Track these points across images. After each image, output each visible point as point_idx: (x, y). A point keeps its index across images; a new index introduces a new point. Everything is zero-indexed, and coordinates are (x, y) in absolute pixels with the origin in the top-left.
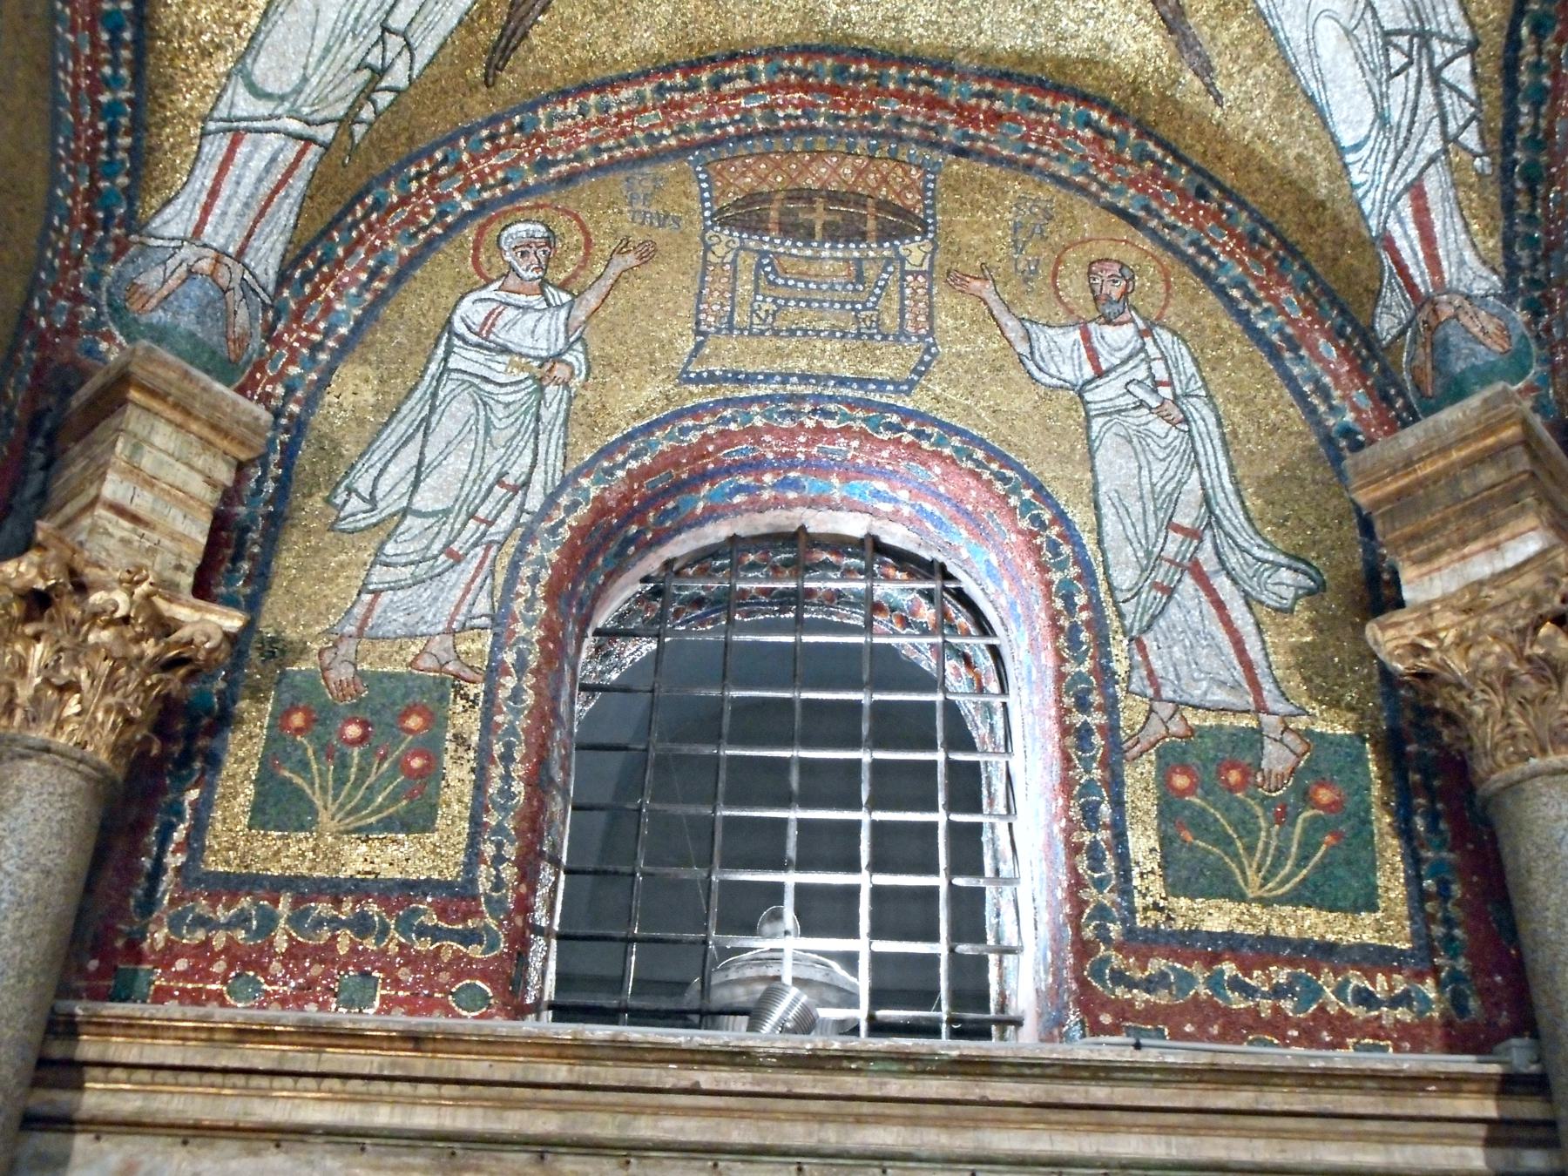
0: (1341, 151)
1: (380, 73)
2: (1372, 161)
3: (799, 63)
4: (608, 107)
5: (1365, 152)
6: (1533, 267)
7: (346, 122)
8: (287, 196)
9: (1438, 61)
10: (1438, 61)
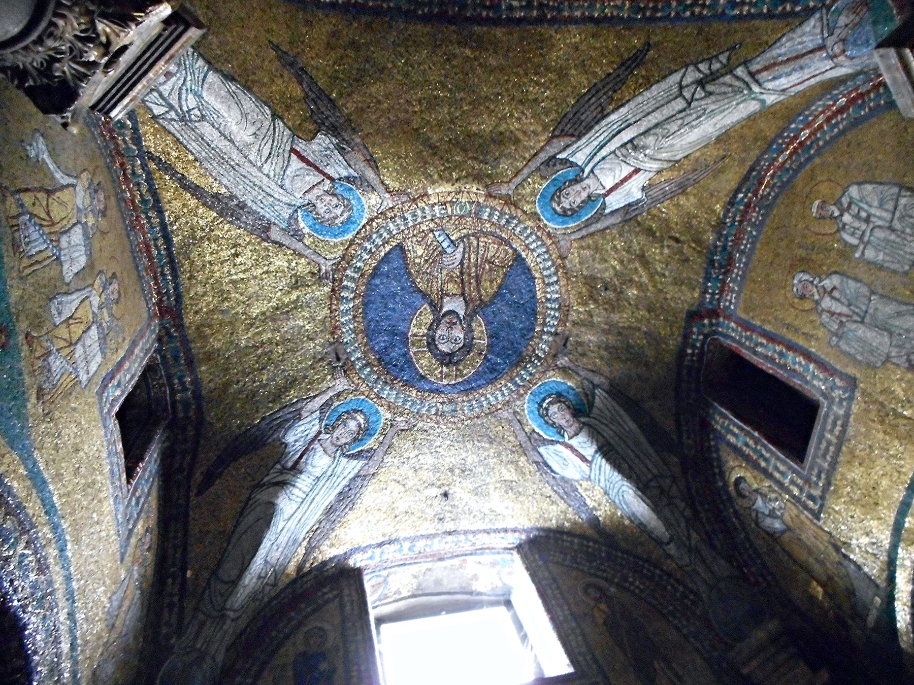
1: (701, 83)
3: (484, 14)
4: (589, 7)
7: (729, 69)
8: (780, 55)
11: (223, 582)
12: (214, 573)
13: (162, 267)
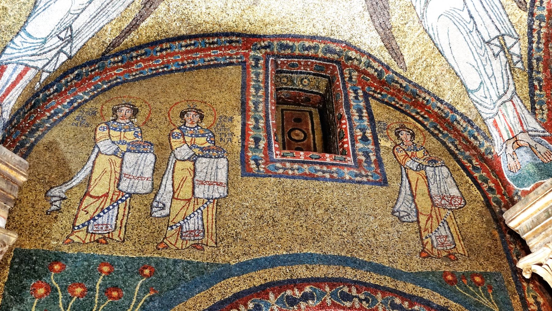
0: (23, 28)
2: (29, 45)
5: (30, 40)
6: (13, 127)
9: (64, 49)
10: (64, 49)
11: (476, 90)
12: (467, 91)
13: (206, 43)
